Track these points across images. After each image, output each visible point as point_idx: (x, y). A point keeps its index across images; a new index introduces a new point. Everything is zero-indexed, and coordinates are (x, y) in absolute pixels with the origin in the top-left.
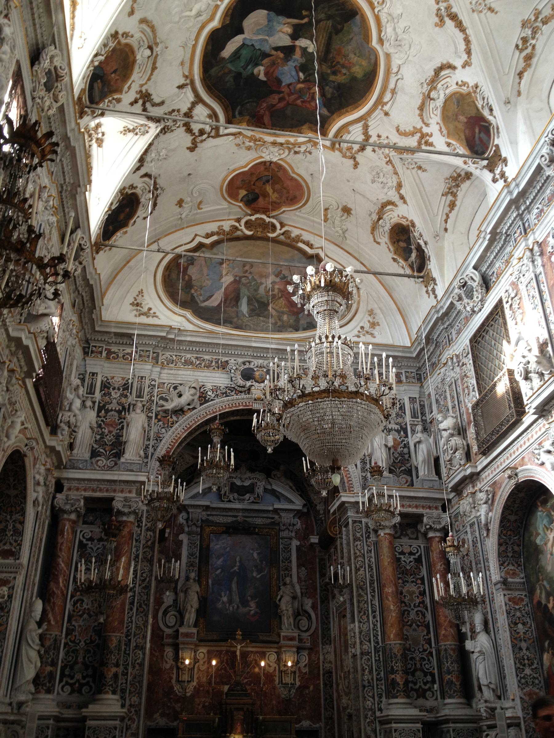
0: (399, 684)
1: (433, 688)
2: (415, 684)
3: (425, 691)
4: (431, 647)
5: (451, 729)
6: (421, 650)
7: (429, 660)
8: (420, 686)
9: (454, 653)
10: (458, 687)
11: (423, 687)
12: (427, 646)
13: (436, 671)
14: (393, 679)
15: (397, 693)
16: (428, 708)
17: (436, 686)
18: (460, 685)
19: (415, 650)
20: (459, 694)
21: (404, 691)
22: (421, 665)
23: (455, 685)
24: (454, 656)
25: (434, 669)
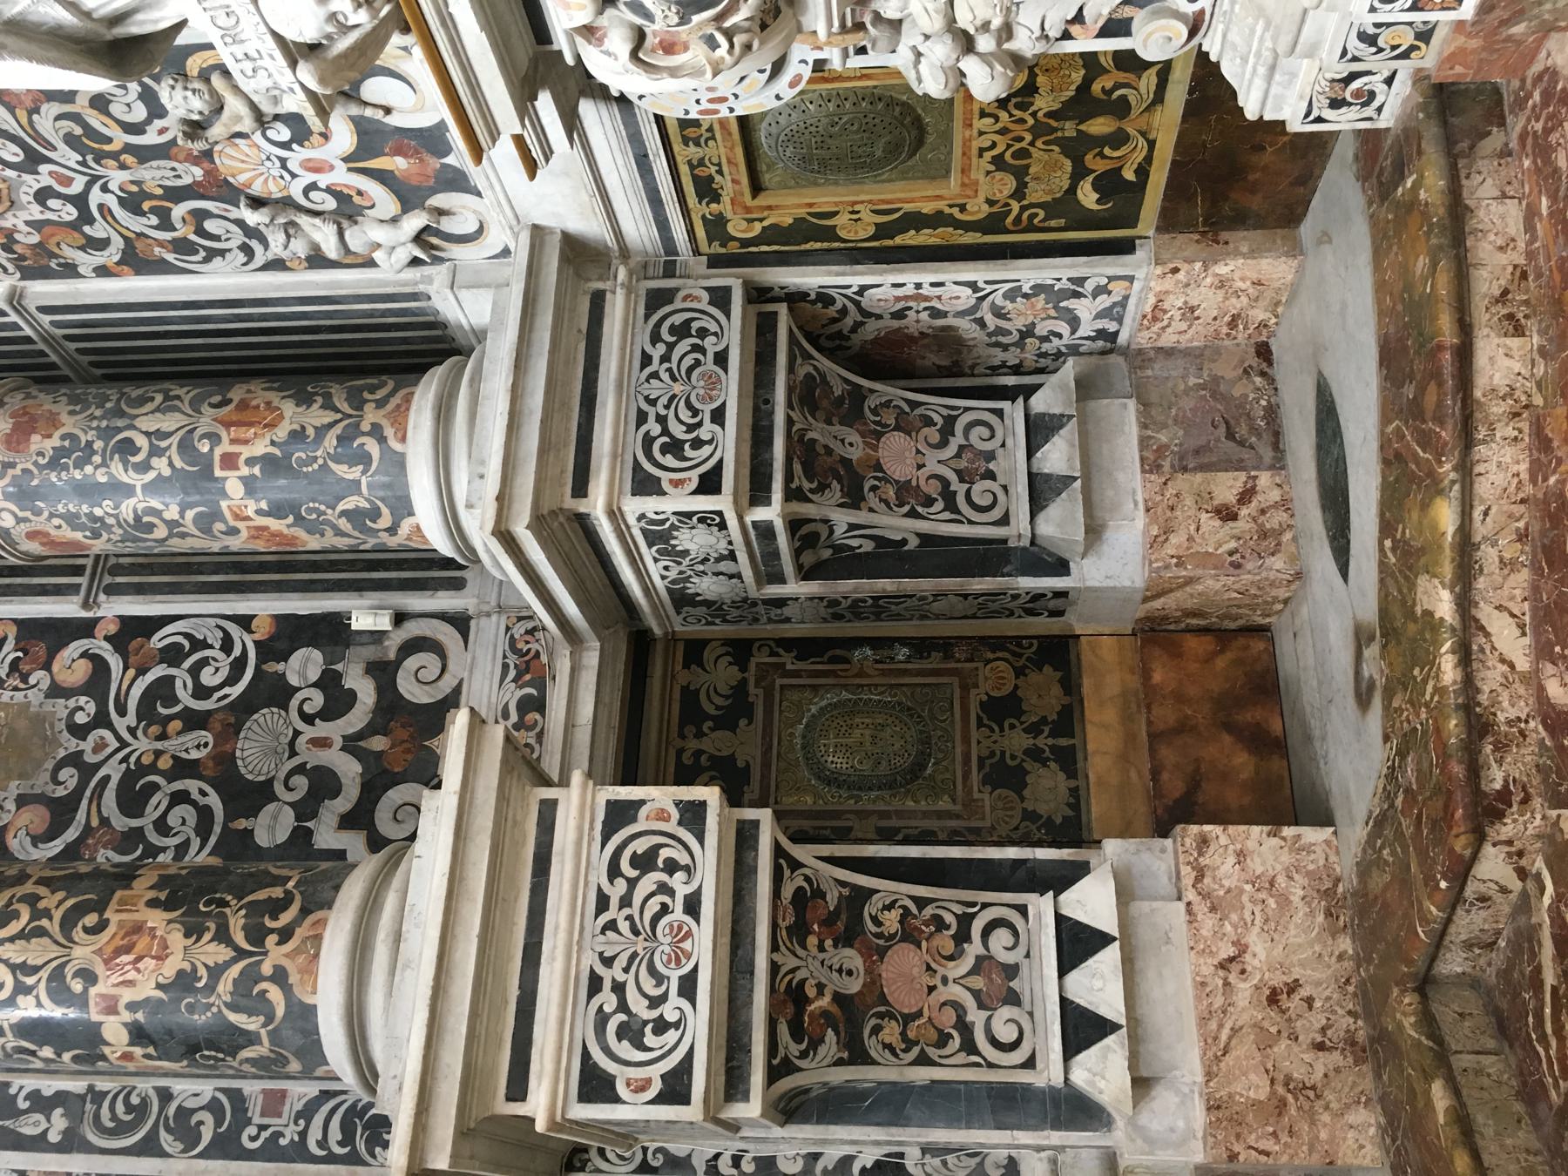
0: (183, 982)
1: (377, 636)
2: (324, 784)
3: (391, 706)
4: (86, 628)
5: (634, 507)
6: (87, 708)
7: (173, 655)
8: (351, 744)
9: (54, 422)
10: (316, 416)
11: (356, 720)
12: (71, 664)
13: (265, 607)
14: (138, 1034)
15: (260, 1005)
16: (513, 695)
17: (366, 616)
18: (304, 400)
19: (75, 759)
20: (371, 415)
21: (257, 935)
22: (194, 720)
23: (298, 435)
24: (69, 424)
25: (245, 622)
